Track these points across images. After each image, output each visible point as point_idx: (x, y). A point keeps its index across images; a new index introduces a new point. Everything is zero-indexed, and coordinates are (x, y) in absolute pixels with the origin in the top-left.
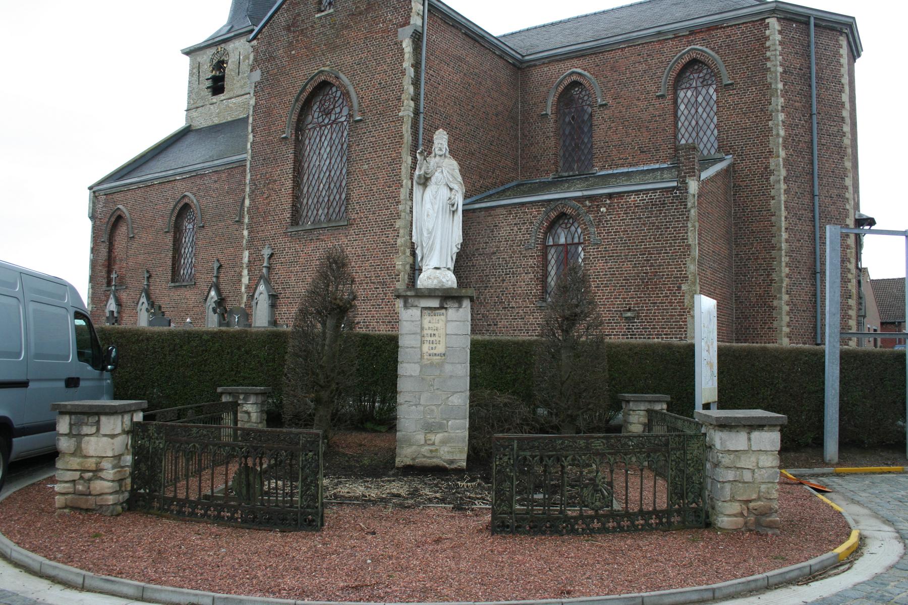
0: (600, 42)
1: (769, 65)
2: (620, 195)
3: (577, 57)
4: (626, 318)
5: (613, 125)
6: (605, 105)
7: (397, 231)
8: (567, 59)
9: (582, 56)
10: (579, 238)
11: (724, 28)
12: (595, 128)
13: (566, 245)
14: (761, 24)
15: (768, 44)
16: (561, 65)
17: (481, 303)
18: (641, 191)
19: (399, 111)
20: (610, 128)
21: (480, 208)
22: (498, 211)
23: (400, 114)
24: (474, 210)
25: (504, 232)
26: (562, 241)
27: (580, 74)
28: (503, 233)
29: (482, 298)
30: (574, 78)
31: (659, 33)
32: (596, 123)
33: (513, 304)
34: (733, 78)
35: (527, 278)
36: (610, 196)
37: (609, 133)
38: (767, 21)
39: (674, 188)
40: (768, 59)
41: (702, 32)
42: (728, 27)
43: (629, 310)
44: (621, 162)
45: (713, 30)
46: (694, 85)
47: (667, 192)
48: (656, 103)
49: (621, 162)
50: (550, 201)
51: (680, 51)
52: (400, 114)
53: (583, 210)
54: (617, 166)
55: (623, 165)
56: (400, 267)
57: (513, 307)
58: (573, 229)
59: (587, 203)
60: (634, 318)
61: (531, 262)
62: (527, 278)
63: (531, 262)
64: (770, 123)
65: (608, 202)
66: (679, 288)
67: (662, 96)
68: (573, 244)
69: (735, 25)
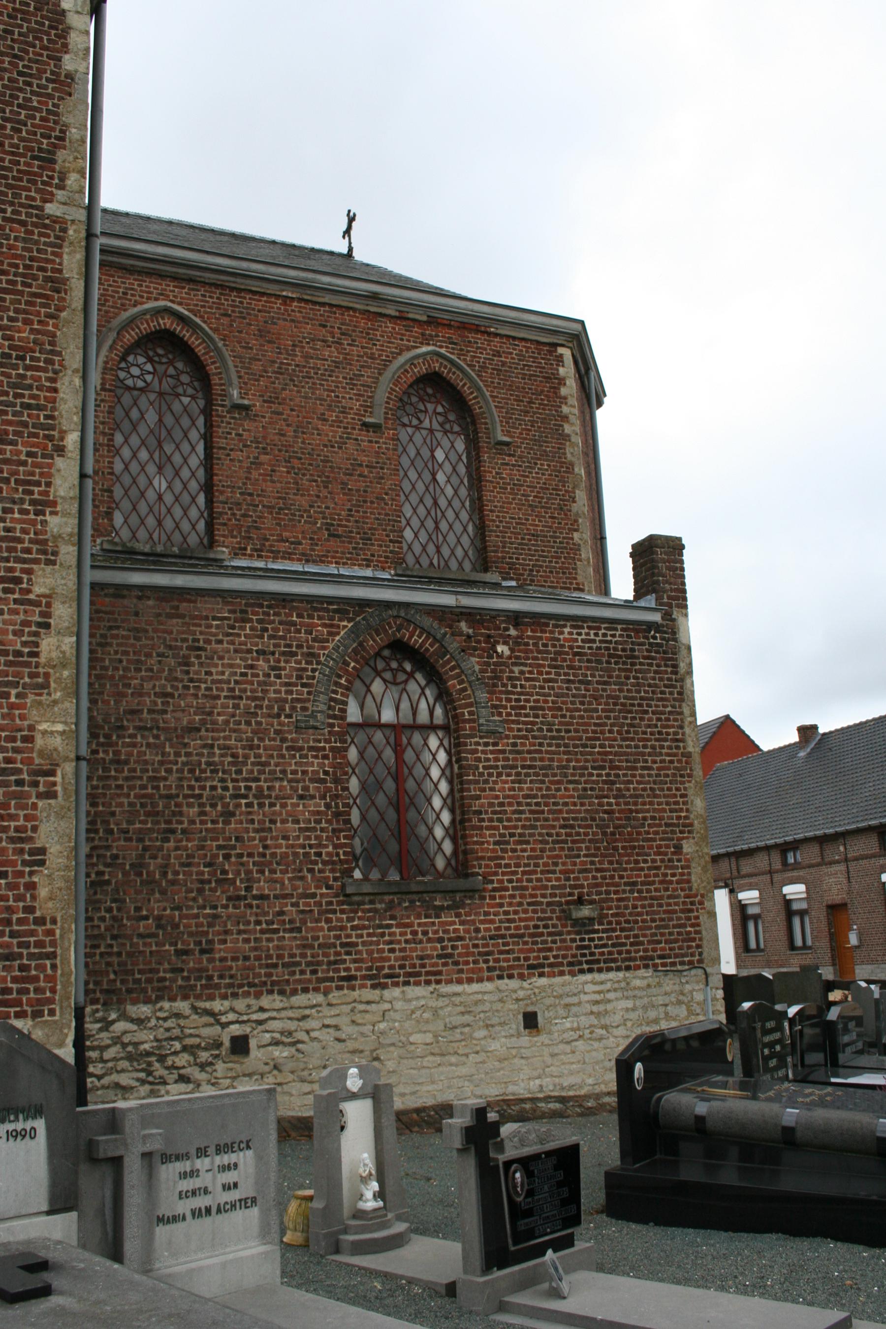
0: (244, 265)
1: (568, 429)
2: (538, 620)
3: (175, 278)
4: (577, 922)
5: (264, 458)
6: (246, 408)
7: (45, 604)
8: (150, 273)
9: (191, 280)
10: (431, 713)
11: (489, 334)
12: (221, 454)
13: (397, 729)
14: (550, 352)
15: (563, 391)
16: (132, 282)
17: (150, 882)
18: (584, 619)
19: (48, 198)
20: (257, 464)
21: (142, 588)
22: (204, 606)
23: (51, 208)
24: (121, 591)
25: (225, 669)
26: (388, 716)
27: (181, 318)
28: (221, 671)
29: (153, 865)
30: (166, 322)
31: (374, 297)
32: (222, 443)
33: (262, 886)
34: (508, 433)
35: (306, 810)
36: (517, 618)
37: (255, 475)
38: (561, 350)
39: (650, 625)
40: (565, 418)
41: (449, 326)
42: (496, 335)
43: (580, 901)
44: (283, 547)
45: (470, 330)
46: (426, 424)
47: (637, 631)
48: (364, 437)
49: (283, 547)
50: (363, 604)
51: (409, 349)
52: (51, 208)
53: (453, 645)
54: (276, 555)
55: (288, 556)
56: (57, 741)
57: (262, 897)
58: (412, 687)
59: (463, 625)
60: (591, 920)
61: (314, 765)
62: (306, 810)
63: (314, 765)
64: (576, 535)
65: (513, 632)
66: (678, 849)
67: (376, 427)
68: (415, 727)
69: (508, 337)
